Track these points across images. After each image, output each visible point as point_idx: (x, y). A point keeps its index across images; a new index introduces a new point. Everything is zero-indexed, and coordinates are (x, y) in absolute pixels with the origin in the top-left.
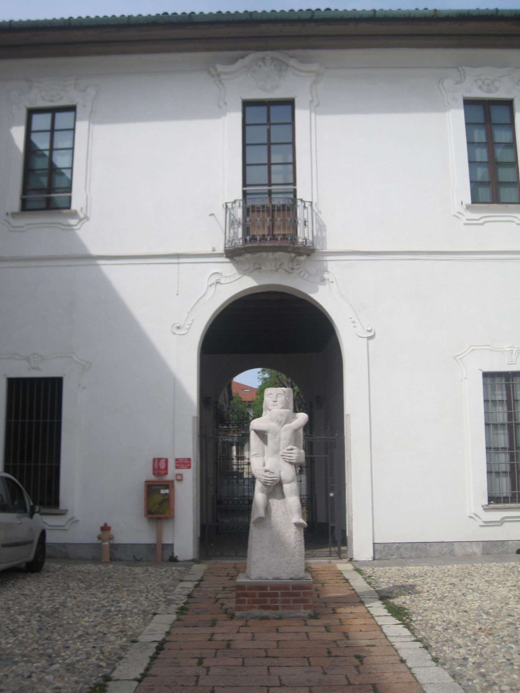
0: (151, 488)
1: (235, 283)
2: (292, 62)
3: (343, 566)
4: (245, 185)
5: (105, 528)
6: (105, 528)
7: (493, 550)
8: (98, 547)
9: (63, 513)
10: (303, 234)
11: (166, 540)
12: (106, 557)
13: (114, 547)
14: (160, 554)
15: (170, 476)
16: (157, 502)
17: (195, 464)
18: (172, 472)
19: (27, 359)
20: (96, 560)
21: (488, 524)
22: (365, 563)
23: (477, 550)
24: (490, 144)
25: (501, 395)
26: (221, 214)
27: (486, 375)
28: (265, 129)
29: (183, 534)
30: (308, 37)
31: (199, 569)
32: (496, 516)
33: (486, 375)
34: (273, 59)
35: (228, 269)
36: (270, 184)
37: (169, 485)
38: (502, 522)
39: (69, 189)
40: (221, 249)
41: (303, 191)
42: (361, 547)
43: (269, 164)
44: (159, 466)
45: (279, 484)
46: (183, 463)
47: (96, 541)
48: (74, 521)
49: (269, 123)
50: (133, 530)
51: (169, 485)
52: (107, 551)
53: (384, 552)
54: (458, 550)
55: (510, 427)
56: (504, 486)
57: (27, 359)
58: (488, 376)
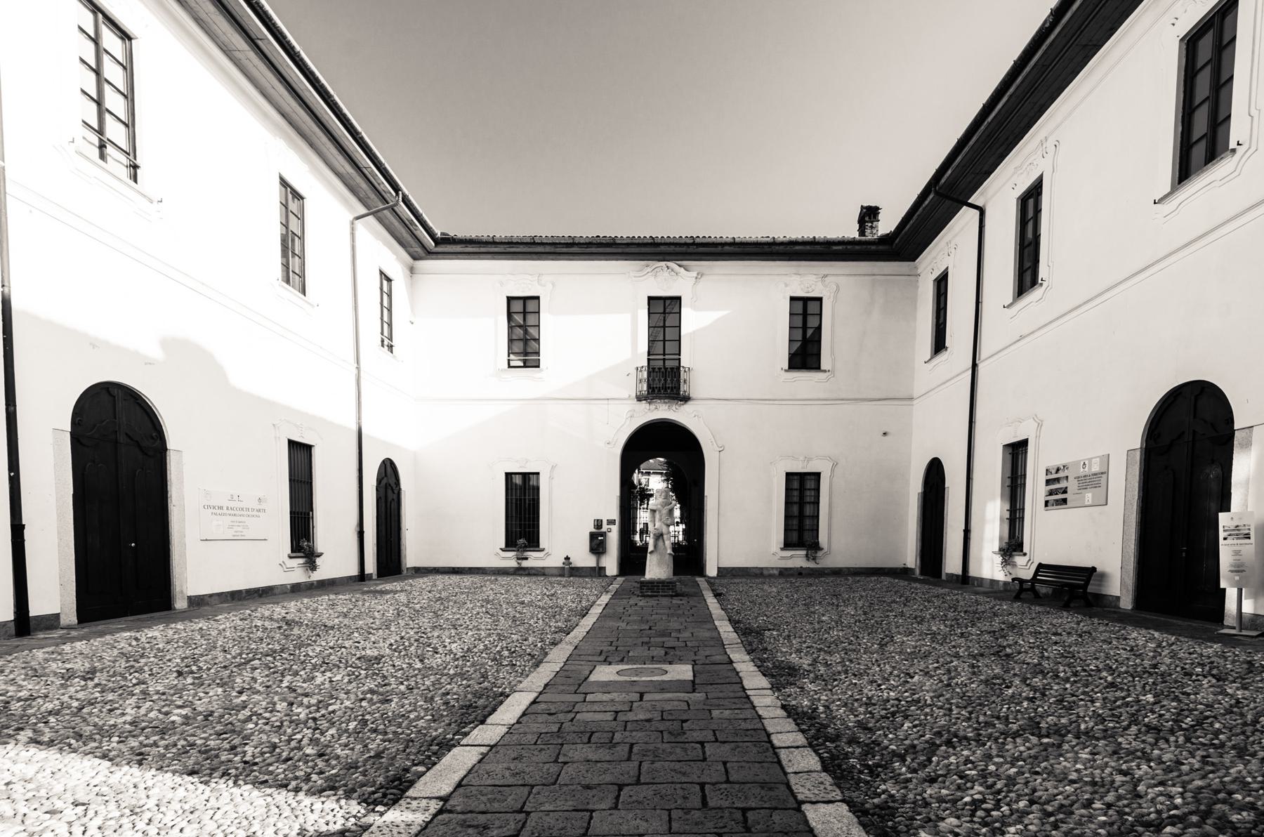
0: (593, 536)
5: (567, 558)
6: (567, 558)
7: (784, 573)
8: (563, 568)
9: (543, 550)
10: (683, 388)
12: (566, 572)
14: (599, 572)
15: (604, 529)
16: (597, 544)
18: (605, 528)
20: (562, 575)
25: (796, 485)
29: (611, 563)
30: (691, 254)
31: (620, 579)
37: (603, 534)
39: (538, 354)
41: (685, 362)
42: (711, 571)
43: (664, 327)
44: (598, 524)
45: (662, 535)
46: (611, 522)
48: (548, 554)
50: (584, 559)
51: (603, 534)
52: (570, 571)
54: (765, 572)
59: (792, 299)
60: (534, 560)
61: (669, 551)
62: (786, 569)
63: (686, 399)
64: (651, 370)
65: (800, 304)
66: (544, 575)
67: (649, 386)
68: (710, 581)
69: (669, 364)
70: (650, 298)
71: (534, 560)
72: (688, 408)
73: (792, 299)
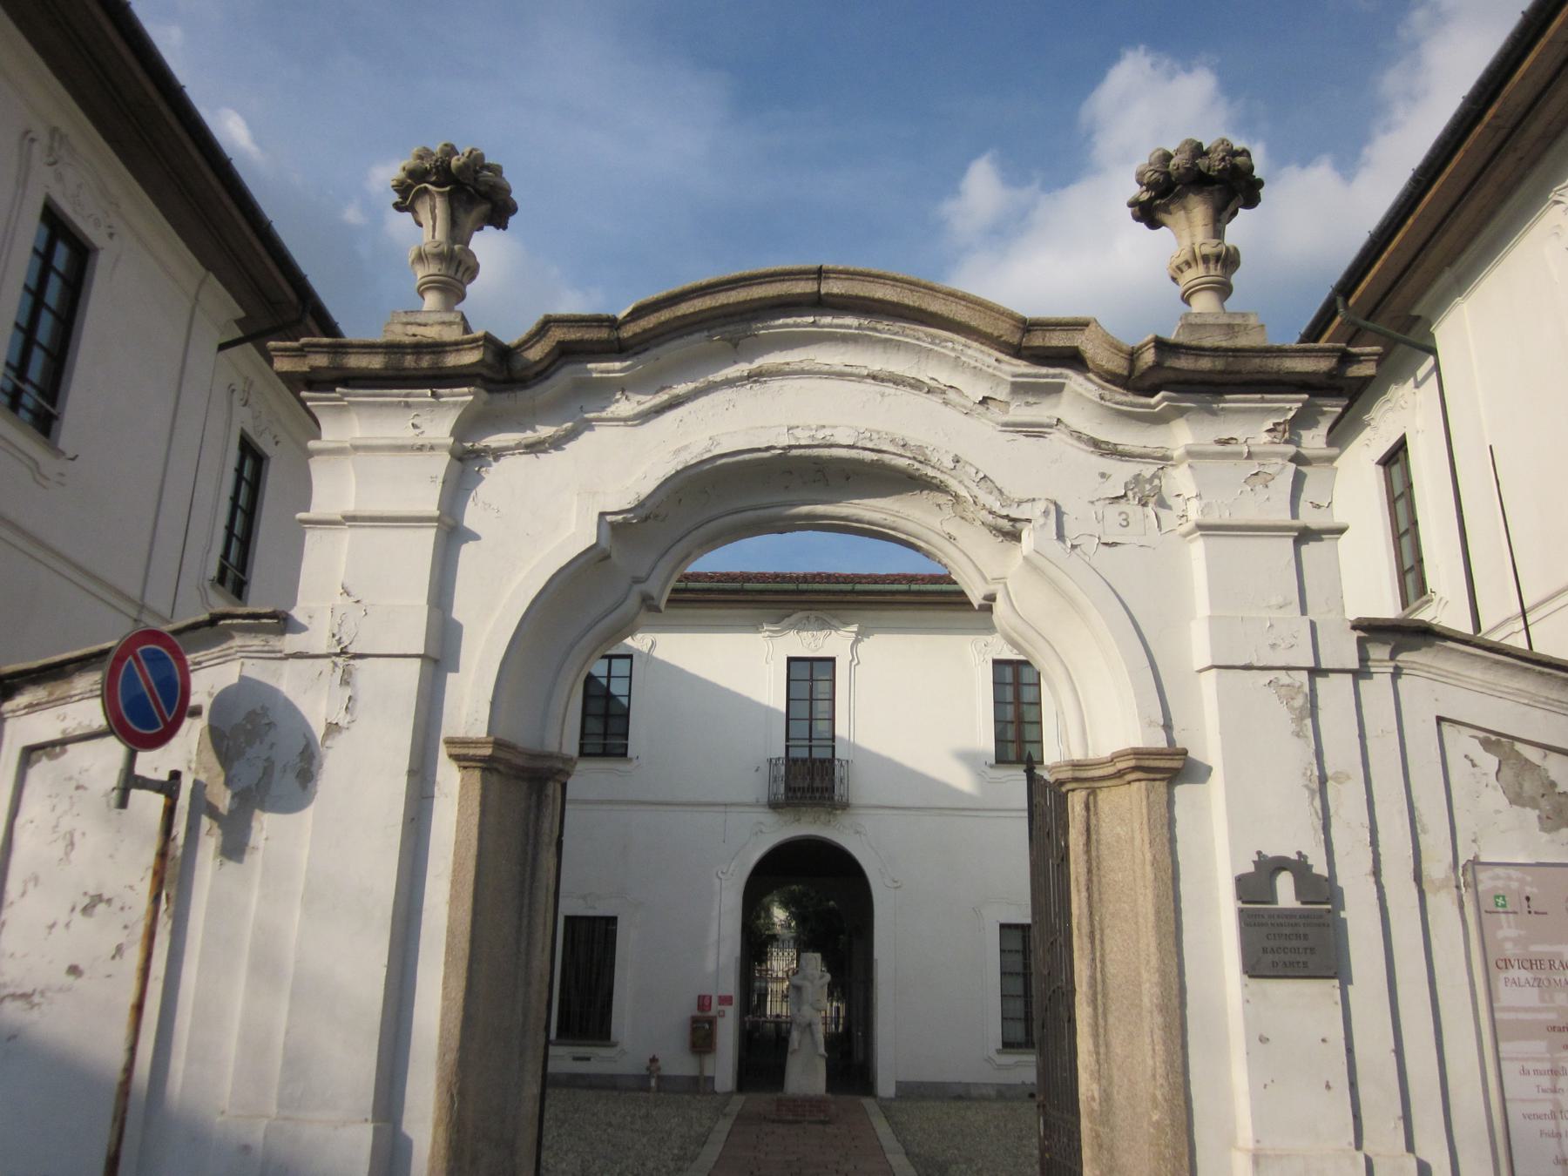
1: (777, 831)
2: (835, 622)
3: (867, 1102)
4: (787, 739)
5: (654, 1060)
6: (654, 1060)
8: (647, 1078)
9: (614, 1045)
11: (708, 1073)
13: (661, 1078)
14: (699, 1085)
15: (713, 1012)
16: (701, 1037)
17: (736, 1000)
19: (584, 898)
20: (648, 1089)
21: (1000, 1067)
22: (891, 1100)
23: (993, 1093)
24: (1018, 701)
25: (1017, 944)
26: (765, 768)
27: (1003, 926)
28: (807, 684)
29: (723, 1066)
31: (739, 1101)
32: (1010, 1059)
33: (1003, 926)
34: (817, 618)
35: (769, 818)
36: (810, 739)
38: (1017, 1064)
40: (765, 800)
42: (885, 1085)
44: (703, 1002)
45: (810, 1025)
46: (725, 1000)
47: (644, 1072)
49: (812, 680)
50: (678, 1063)
51: (712, 1022)
53: (911, 1092)
55: (1025, 975)
56: (1018, 1032)
57: (584, 898)
58: (1004, 927)
59: (996, 663)
60: (600, 1061)
61: (822, 1050)
62: (1009, 1086)
63: (845, 806)
64: (790, 762)
65: (1008, 672)
66: (614, 1088)
67: (788, 788)
68: (886, 1108)
69: (818, 753)
70: (790, 660)
71: (600, 1061)
72: (844, 819)
73: (996, 663)
